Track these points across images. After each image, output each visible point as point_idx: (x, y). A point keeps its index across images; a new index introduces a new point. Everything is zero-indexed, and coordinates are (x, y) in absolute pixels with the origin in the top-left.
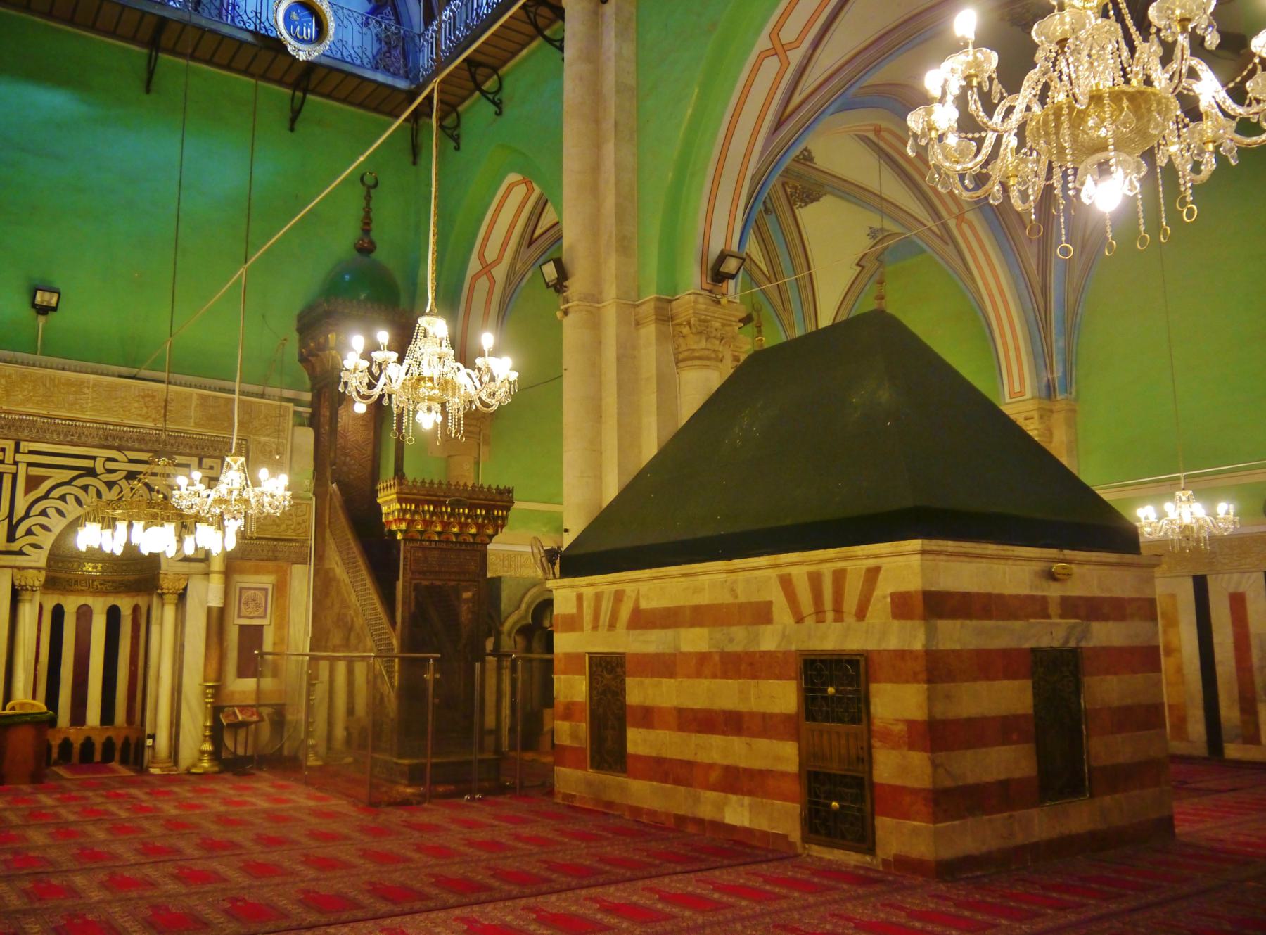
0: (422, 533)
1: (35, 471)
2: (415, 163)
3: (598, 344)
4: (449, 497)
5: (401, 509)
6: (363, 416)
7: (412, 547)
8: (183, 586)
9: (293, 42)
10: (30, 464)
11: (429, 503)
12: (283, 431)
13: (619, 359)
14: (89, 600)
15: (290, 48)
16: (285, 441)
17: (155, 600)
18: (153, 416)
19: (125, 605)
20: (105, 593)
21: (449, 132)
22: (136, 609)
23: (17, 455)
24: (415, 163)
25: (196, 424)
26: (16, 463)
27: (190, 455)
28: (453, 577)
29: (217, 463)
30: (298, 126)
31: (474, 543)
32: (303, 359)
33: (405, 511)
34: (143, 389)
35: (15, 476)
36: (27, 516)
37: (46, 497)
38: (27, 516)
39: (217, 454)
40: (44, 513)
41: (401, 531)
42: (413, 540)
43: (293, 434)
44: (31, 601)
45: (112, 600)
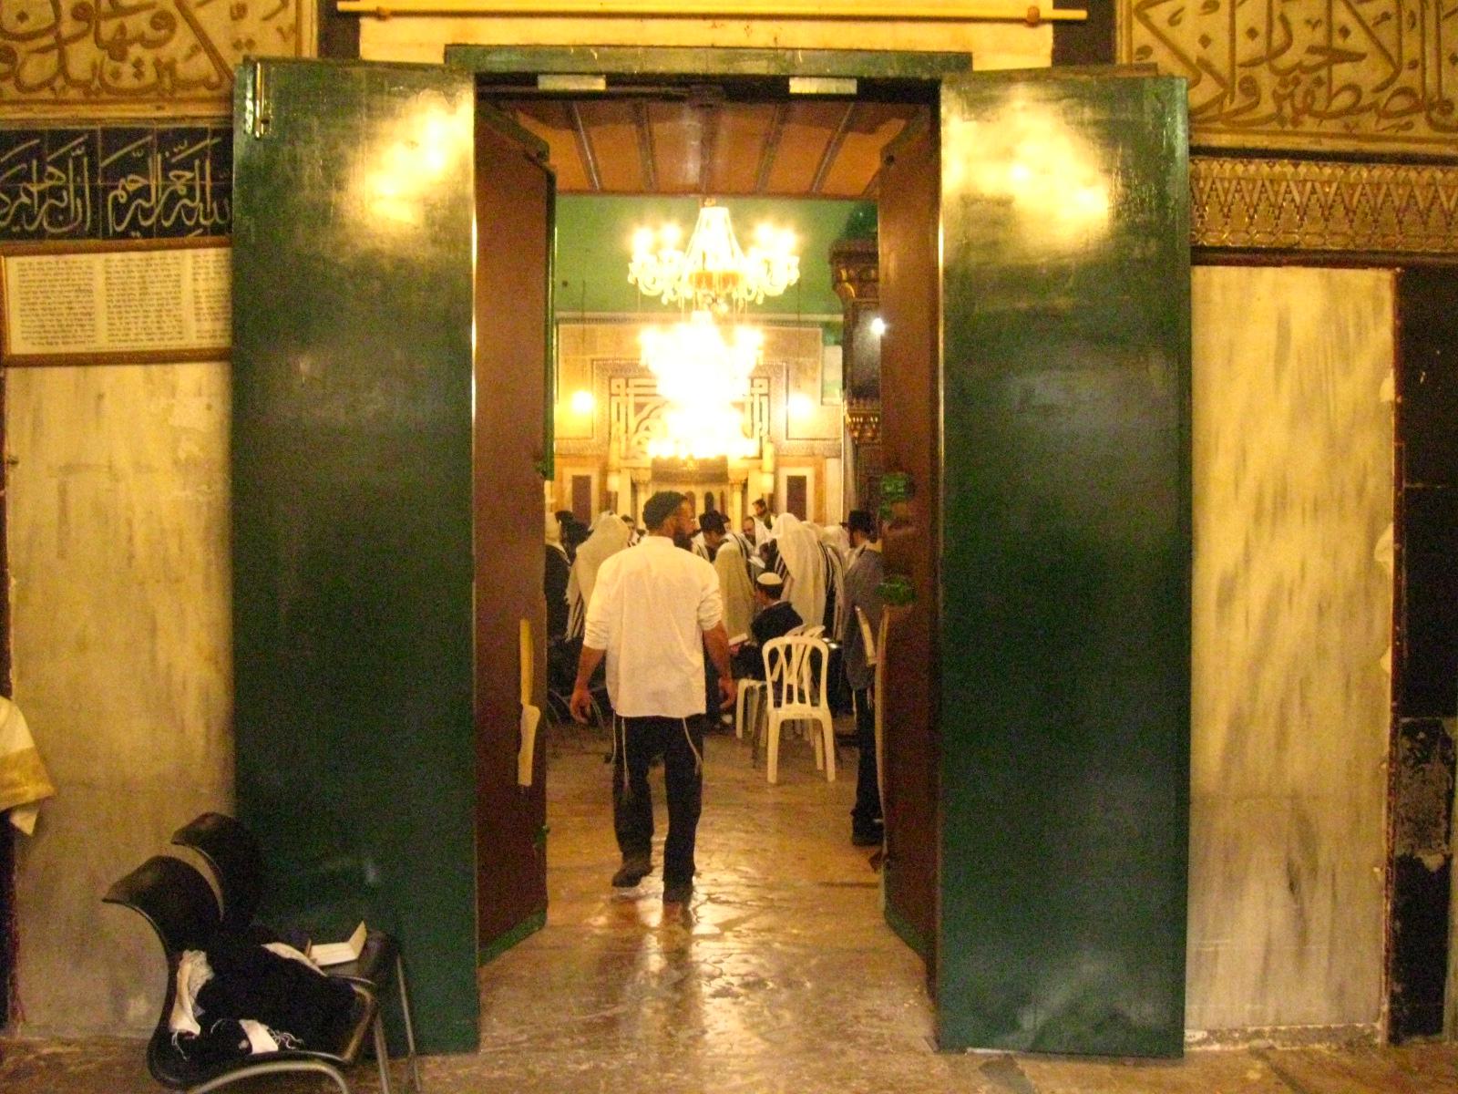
0: (873, 438)
1: (641, 400)
8: (744, 478)
10: (636, 395)
11: (874, 416)
12: (816, 351)
14: (693, 489)
17: (728, 488)
19: (716, 491)
20: (703, 483)
22: (722, 496)
26: (627, 395)
32: (834, 287)
33: (856, 424)
36: (637, 431)
37: (648, 417)
38: (637, 431)
39: (764, 375)
40: (647, 429)
42: (865, 444)
43: (823, 352)
44: (646, 491)
45: (707, 488)
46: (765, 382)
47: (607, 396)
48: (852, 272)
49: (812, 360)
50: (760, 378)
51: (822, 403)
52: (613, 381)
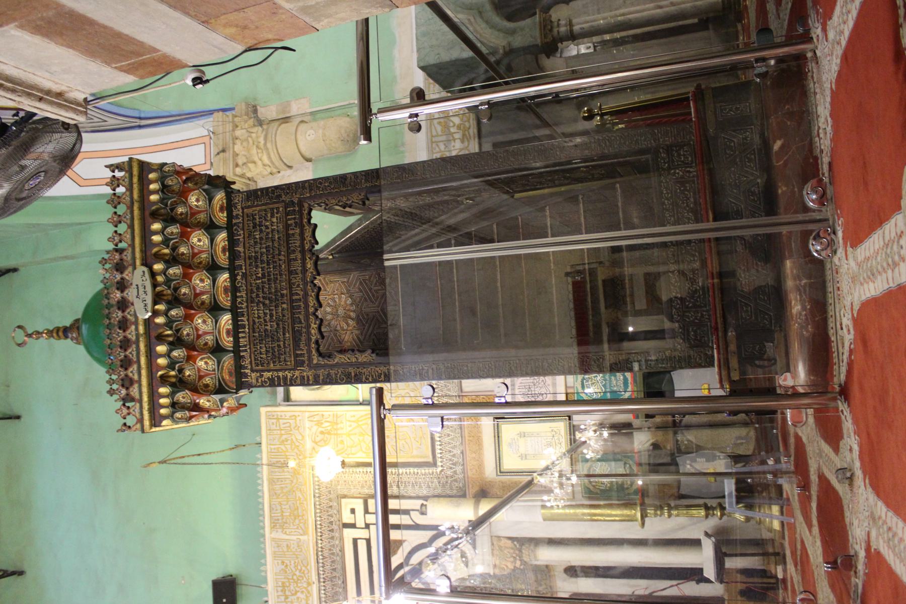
5: (171, 416)
7: (252, 371)
8: (509, 542)
16: (307, 414)
18: (305, 585)
25: (305, 533)
27: (342, 539)
28: (297, 266)
31: (229, 227)
33: (174, 405)
34: (278, 596)
41: (222, 401)
46: (347, 504)
49: (307, 424)
50: (339, 512)
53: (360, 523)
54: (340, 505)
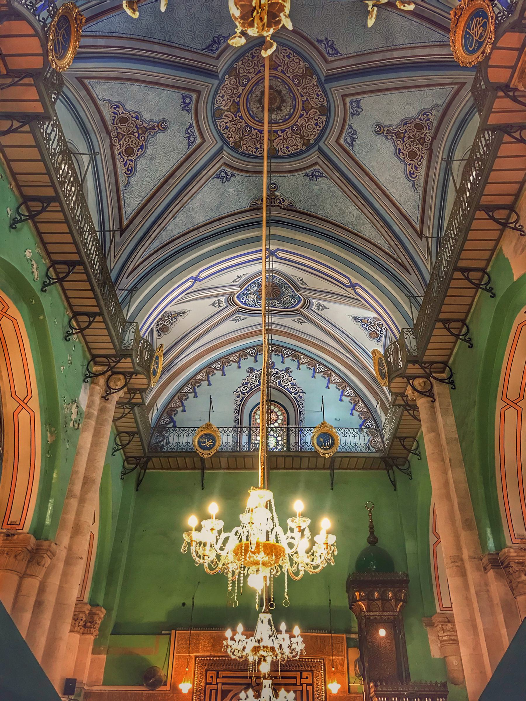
1: (225, 687)
2: (395, 490)
3: (466, 587)
4: (406, 691)
6: (387, 637)
9: (322, 451)
13: (477, 594)
15: (321, 454)
21: (405, 471)
23: (218, 679)
24: (395, 490)
29: (309, 675)
30: (334, 487)
32: (351, 608)
35: (217, 690)
47: (203, 684)
48: (363, 594)
50: (307, 671)
51: (349, 692)
52: (208, 672)
53: (303, 681)
54: (309, 671)
